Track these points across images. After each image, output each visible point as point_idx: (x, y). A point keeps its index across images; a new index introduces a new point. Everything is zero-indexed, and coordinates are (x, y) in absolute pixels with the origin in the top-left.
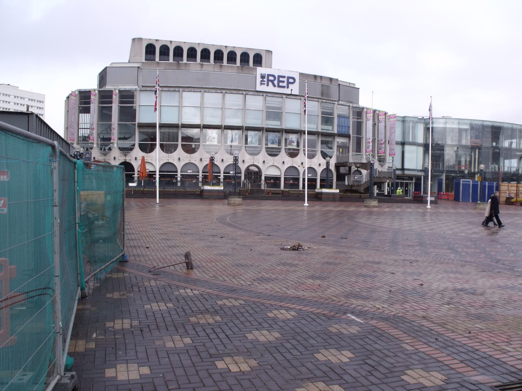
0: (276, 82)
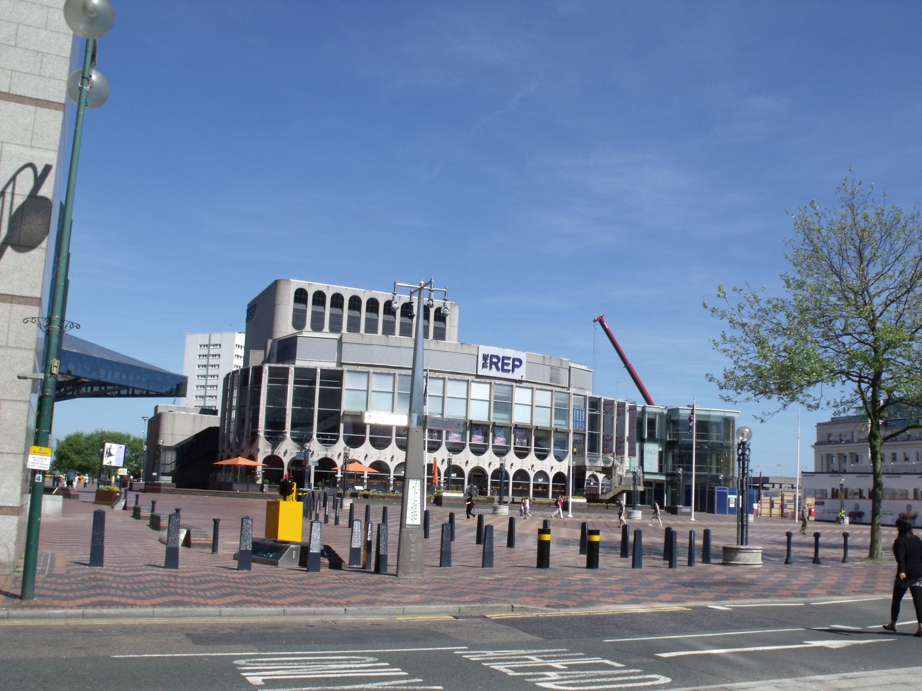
0: (500, 365)
